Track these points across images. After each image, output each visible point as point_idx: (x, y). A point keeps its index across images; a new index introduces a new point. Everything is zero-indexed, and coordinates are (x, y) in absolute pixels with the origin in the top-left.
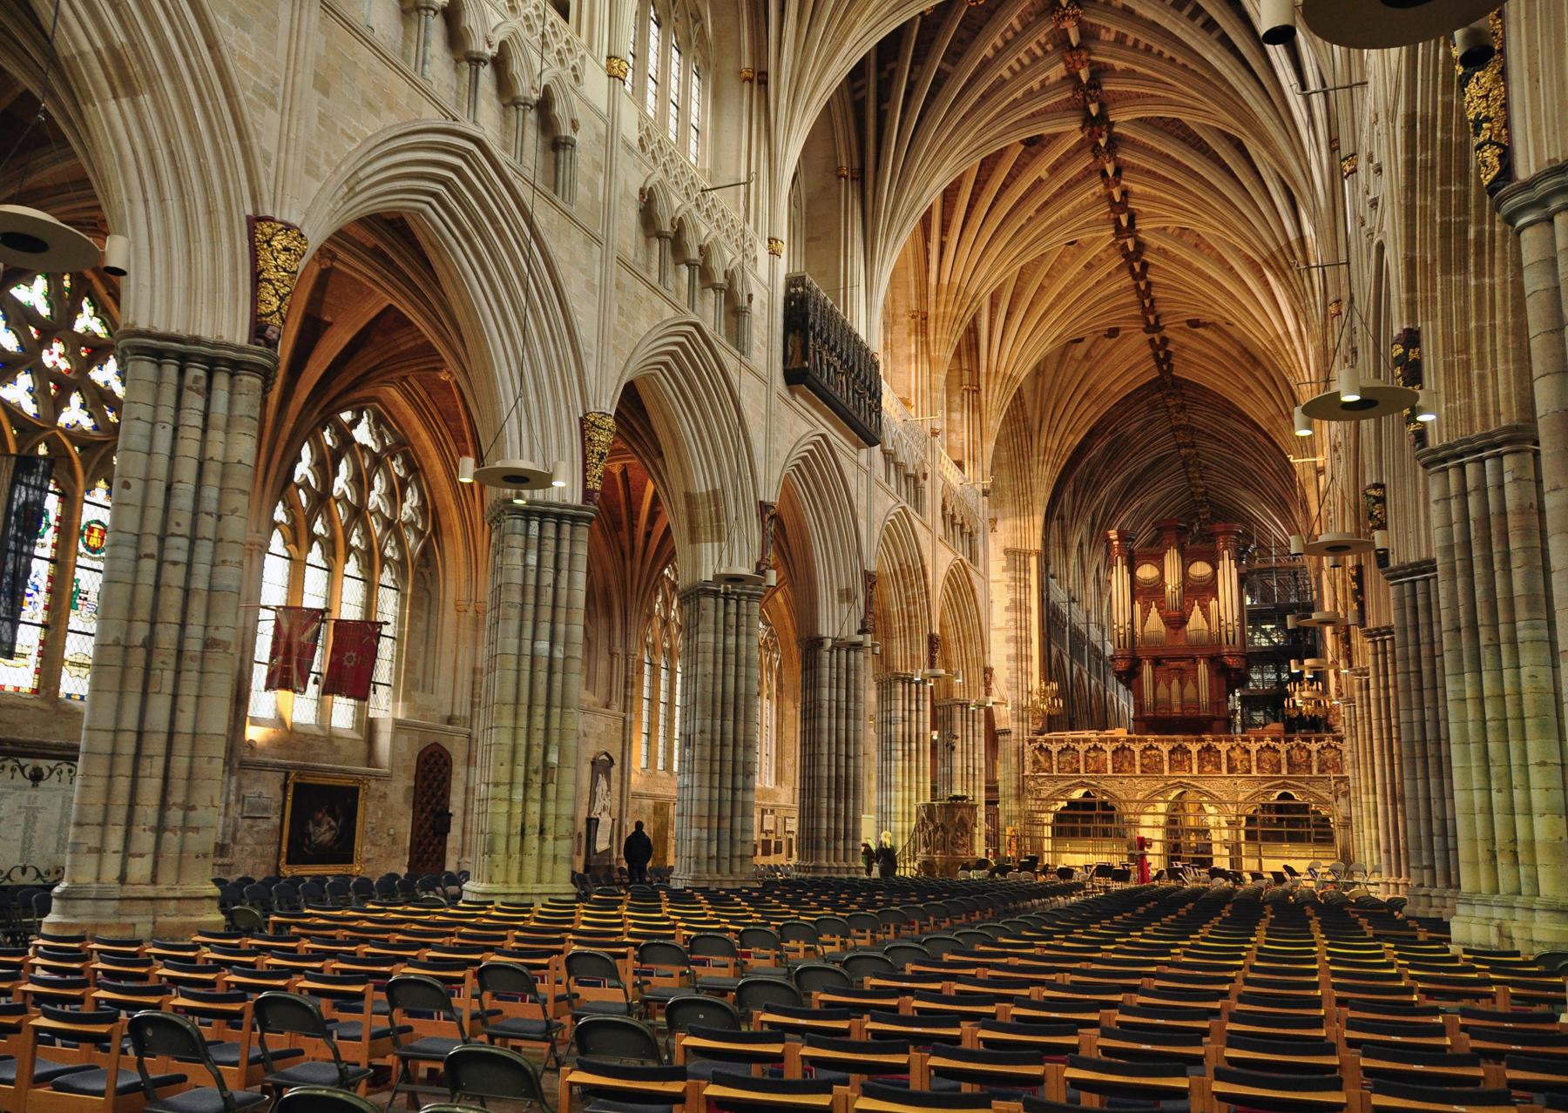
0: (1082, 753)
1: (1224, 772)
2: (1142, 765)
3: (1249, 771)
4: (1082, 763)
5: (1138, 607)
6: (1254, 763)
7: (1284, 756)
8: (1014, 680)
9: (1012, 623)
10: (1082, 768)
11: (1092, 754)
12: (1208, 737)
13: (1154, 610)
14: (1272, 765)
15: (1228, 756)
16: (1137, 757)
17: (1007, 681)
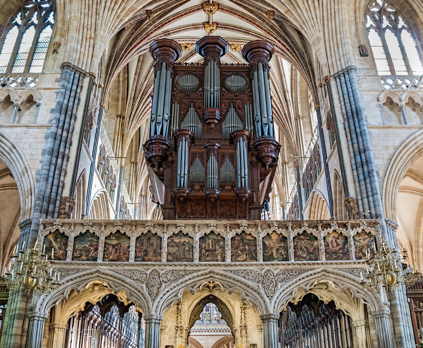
0: (102, 238)
1: (261, 262)
2: (169, 254)
3: (287, 259)
4: (101, 248)
5: (177, 106)
6: (291, 251)
7: (322, 242)
8: (45, 172)
9: (54, 122)
10: (100, 255)
11: (114, 242)
12: (244, 222)
13: (192, 110)
14: (309, 253)
15: (264, 244)
16: (165, 244)
17: (38, 173)
